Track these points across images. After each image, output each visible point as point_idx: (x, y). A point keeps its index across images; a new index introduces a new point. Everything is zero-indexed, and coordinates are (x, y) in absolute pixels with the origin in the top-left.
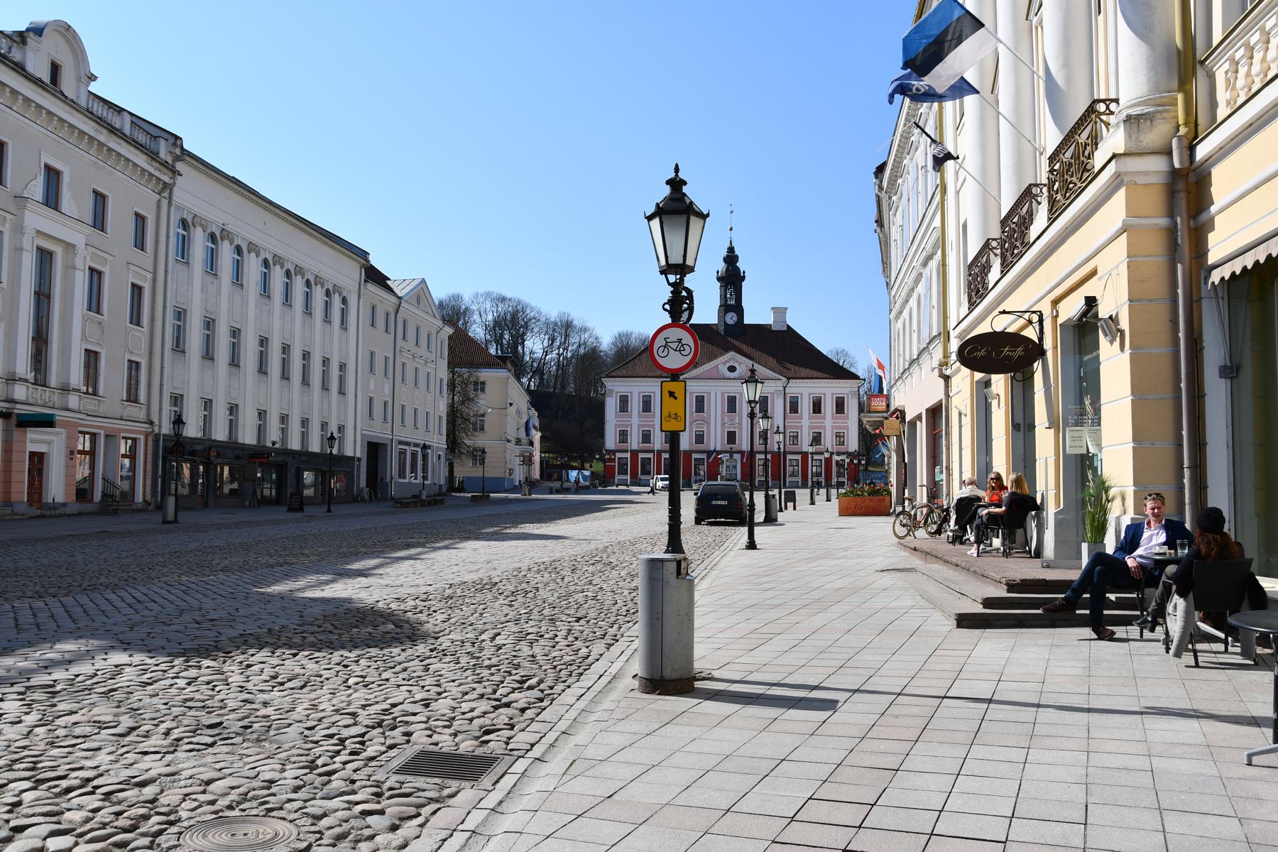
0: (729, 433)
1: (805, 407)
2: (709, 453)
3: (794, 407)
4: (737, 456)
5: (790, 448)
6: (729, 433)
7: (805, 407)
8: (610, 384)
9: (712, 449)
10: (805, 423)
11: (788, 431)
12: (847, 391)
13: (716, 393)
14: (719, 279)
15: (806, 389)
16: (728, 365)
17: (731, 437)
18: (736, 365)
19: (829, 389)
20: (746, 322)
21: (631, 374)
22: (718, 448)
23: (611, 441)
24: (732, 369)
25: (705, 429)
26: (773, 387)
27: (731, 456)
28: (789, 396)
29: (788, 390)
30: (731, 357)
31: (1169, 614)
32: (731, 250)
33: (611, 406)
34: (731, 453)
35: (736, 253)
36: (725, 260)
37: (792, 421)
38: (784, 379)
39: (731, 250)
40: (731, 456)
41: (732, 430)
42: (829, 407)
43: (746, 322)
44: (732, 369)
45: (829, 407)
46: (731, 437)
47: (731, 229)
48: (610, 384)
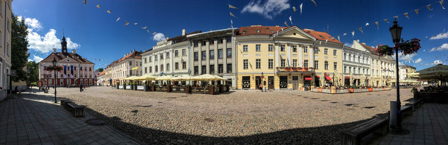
1: (83, 69)
2: (64, 79)
3: (81, 69)
4: (70, 80)
5: (81, 78)
9: (65, 78)
11: (80, 74)
12: (92, 66)
15: (83, 65)
16: (68, 60)
21: (47, 61)
24: (68, 61)
27: (69, 80)
31: (125, 122)
34: (69, 79)
37: (81, 72)
40: (69, 80)
44: (68, 61)
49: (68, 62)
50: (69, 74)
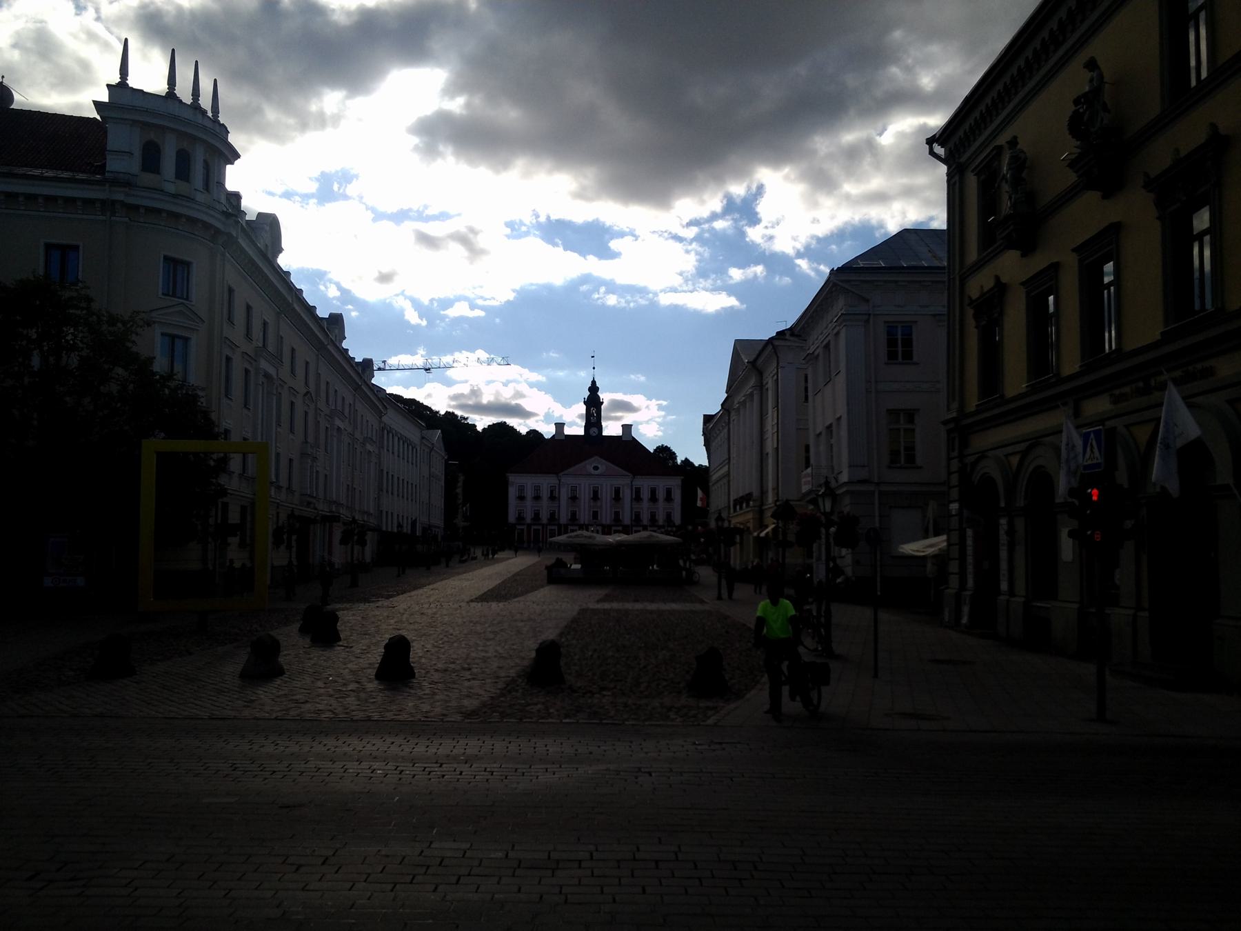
0: (594, 512)
1: (645, 495)
6: (594, 512)
7: (645, 495)
8: (512, 478)
9: (582, 522)
10: (645, 507)
13: (585, 487)
14: (585, 403)
15: (645, 484)
17: (595, 515)
18: (599, 466)
19: (662, 483)
20: (605, 433)
22: (586, 522)
23: (512, 519)
24: (596, 468)
25: (577, 510)
26: (624, 481)
28: (634, 487)
29: (633, 483)
30: (596, 461)
32: (594, 382)
33: (512, 492)
35: (598, 385)
36: (590, 389)
38: (631, 476)
39: (594, 382)
41: (595, 510)
42: (661, 495)
43: (604, 434)
44: (596, 468)
45: (661, 495)
46: (595, 515)
47: (594, 368)
48: (512, 478)
49: (593, 472)
50: (597, 512)
